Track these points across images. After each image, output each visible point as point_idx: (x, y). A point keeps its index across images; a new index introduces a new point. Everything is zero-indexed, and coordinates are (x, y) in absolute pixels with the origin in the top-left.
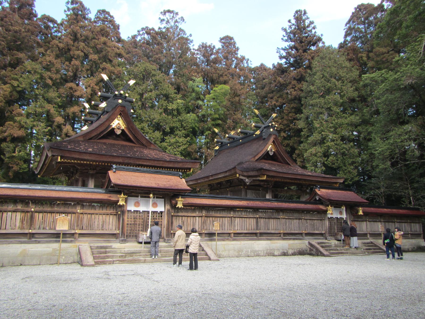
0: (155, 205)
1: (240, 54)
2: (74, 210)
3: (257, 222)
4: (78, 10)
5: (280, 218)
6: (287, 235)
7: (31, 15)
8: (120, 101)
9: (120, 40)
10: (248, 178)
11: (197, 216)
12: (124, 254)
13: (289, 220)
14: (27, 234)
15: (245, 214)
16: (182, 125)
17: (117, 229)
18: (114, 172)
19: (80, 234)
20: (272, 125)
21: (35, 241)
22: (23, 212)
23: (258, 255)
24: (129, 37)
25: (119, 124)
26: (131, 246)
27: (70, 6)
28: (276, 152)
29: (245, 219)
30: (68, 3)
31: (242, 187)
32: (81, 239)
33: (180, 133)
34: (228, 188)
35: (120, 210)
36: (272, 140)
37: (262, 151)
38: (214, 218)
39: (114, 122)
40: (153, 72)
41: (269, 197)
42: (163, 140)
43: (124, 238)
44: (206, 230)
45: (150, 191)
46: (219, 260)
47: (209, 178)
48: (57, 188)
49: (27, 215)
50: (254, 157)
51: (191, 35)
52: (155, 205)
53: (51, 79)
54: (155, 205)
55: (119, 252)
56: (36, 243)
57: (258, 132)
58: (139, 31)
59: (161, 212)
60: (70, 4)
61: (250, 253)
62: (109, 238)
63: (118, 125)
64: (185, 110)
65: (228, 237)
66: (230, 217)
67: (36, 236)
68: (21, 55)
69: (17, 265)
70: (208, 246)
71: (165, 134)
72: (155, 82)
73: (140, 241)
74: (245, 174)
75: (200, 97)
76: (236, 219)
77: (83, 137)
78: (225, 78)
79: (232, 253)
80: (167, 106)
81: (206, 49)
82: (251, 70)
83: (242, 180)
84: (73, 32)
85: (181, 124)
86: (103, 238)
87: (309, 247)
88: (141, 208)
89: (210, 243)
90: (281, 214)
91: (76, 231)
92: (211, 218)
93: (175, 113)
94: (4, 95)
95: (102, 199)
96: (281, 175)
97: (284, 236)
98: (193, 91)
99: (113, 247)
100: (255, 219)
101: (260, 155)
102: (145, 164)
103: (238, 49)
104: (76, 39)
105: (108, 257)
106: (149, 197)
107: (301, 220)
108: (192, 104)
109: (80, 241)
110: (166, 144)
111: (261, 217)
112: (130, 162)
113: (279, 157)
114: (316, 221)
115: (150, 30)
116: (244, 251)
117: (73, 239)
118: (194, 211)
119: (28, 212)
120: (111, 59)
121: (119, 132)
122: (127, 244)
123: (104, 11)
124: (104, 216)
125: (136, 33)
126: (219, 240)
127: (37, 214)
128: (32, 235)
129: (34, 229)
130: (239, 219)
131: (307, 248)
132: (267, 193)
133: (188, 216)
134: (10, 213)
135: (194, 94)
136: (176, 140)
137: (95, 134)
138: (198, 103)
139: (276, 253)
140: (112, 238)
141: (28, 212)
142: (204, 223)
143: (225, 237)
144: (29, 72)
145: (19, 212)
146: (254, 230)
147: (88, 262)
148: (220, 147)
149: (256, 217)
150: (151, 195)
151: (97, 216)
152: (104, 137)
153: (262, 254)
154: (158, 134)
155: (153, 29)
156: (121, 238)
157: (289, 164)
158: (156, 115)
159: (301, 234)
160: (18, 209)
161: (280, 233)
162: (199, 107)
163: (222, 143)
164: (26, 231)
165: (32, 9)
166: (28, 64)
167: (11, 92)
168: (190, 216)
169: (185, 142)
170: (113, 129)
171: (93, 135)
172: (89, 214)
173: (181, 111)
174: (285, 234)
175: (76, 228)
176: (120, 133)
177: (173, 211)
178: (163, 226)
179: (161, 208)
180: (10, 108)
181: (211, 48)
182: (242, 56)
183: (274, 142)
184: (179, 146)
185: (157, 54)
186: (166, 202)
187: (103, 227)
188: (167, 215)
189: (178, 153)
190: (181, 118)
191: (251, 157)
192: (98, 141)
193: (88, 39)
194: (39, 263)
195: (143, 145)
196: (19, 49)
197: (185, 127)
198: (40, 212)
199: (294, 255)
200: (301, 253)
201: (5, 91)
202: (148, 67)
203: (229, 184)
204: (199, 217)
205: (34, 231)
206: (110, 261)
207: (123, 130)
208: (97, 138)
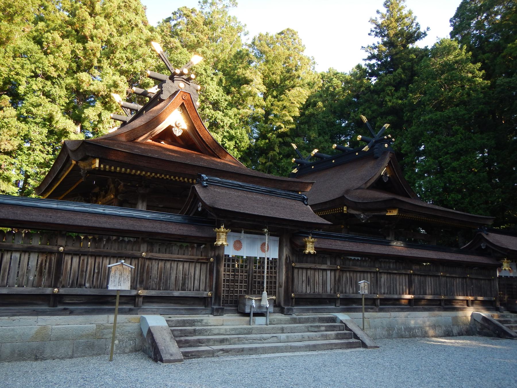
10: (363, 213)
11: (329, 270)
17: (208, 290)
20: (388, 137)
21: (65, 309)
24: (159, 23)
31: (343, 226)
32: (146, 306)
35: (213, 254)
43: (219, 305)
44: (342, 292)
48: (100, 210)
49: (51, 260)
55: (216, 332)
61: (403, 333)
62: (194, 304)
65: (372, 305)
66: (374, 272)
73: (247, 311)
83: (353, 215)
90: (441, 268)
97: (446, 304)
99: (205, 321)
106: (263, 234)
114: (483, 281)
117: (132, 307)
119: (51, 253)
124: (186, 265)
127: (68, 258)
129: (63, 287)
134: (17, 255)
140: (199, 305)
141: (51, 253)
142: (337, 282)
145: (35, 252)
147: (171, 355)
151: (174, 265)
156: (214, 304)
161: (440, 300)
163: (302, 164)
164: (49, 291)
168: (319, 269)
172: (162, 260)
175: (138, 286)
176: (180, 134)
178: (277, 285)
179: (273, 253)
183: (390, 163)
187: (184, 284)
198: (74, 254)
205: (62, 291)
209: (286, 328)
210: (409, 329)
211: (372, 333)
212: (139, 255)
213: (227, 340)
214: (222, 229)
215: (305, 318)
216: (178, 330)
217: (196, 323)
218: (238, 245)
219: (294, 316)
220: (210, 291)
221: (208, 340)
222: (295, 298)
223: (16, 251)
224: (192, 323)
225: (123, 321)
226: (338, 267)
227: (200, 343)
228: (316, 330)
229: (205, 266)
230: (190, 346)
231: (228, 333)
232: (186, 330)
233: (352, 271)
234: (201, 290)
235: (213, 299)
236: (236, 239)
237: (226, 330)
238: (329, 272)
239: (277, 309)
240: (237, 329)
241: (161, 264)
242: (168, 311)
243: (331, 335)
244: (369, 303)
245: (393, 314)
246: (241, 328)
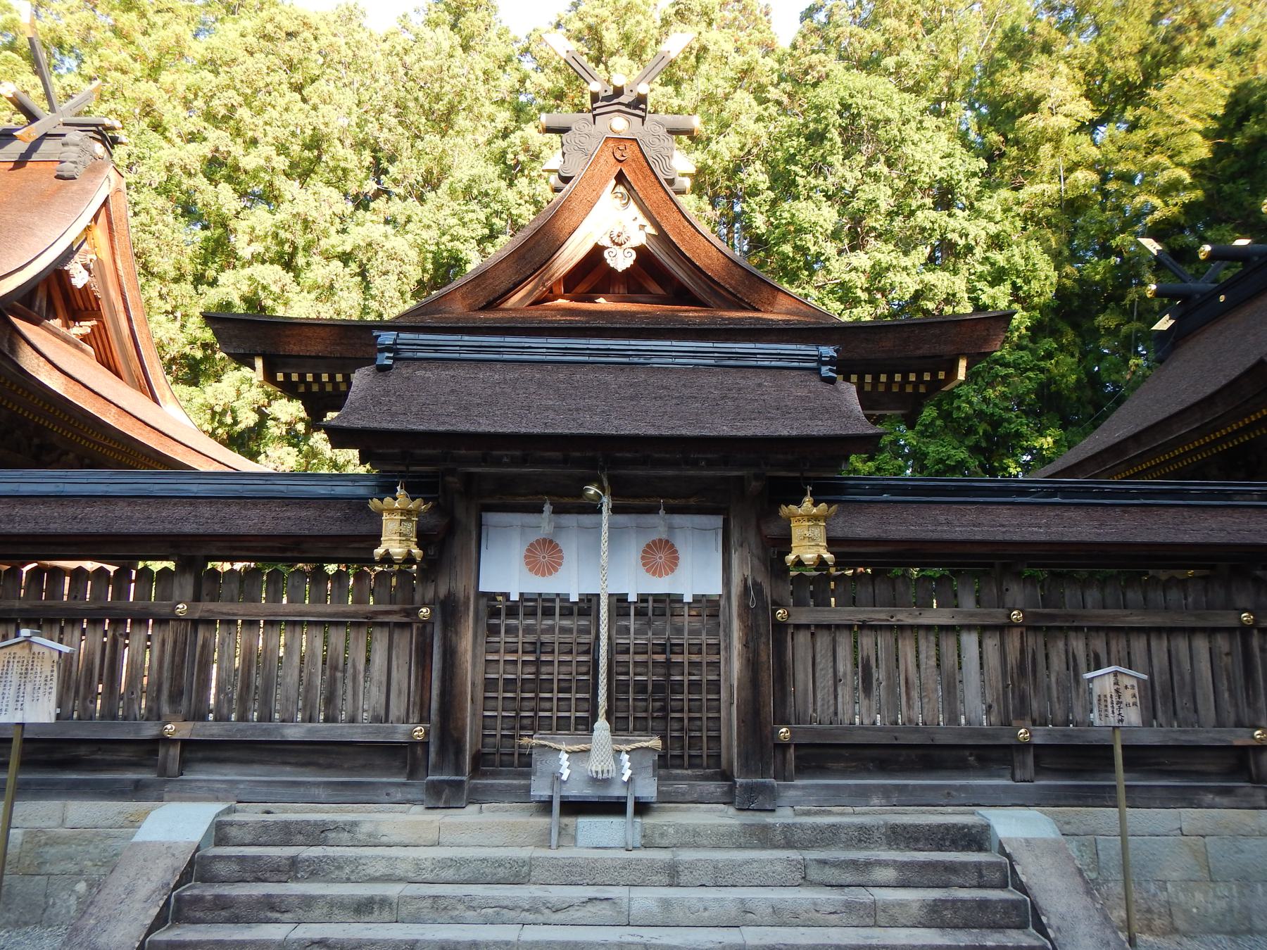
0: (661, 555)
11: (969, 628)
19: (186, 744)
26: (483, 829)
32: (200, 775)
35: (430, 594)
38: (1099, 644)
43: (458, 770)
54: (661, 555)
55: (380, 869)
59: (708, 607)
62: (367, 768)
65: (1232, 774)
66: (1230, 631)
86: (329, 766)
92: (1078, 645)
122: (469, 815)
126: (1137, 798)
133: (902, 628)
140: (388, 770)
156: (439, 768)
163: (1186, 297)
175: (166, 709)
178: (724, 695)
186: (734, 539)
187: (330, 700)
209: (692, 866)
211: (1222, 905)
212: (168, 610)
213: (384, 902)
215: (814, 828)
216: (229, 858)
217: (332, 835)
218: (544, 555)
219: (783, 817)
220: (421, 721)
221: (307, 902)
222: (796, 745)
224: (318, 834)
225: (110, 822)
226: (1016, 616)
227: (272, 908)
228: (848, 877)
229: (407, 634)
230: (235, 920)
231: (429, 877)
232: (259, 858)
233: (1097, 629)
234: (391, 717)
235: (432, 749)
237: (417, 864)
238: (970, 641)
239: (713, 787)
240: (467, 862)
242: (264, 789)
243: (902, 904)
244: (1212, 768)
246: (484, 860)
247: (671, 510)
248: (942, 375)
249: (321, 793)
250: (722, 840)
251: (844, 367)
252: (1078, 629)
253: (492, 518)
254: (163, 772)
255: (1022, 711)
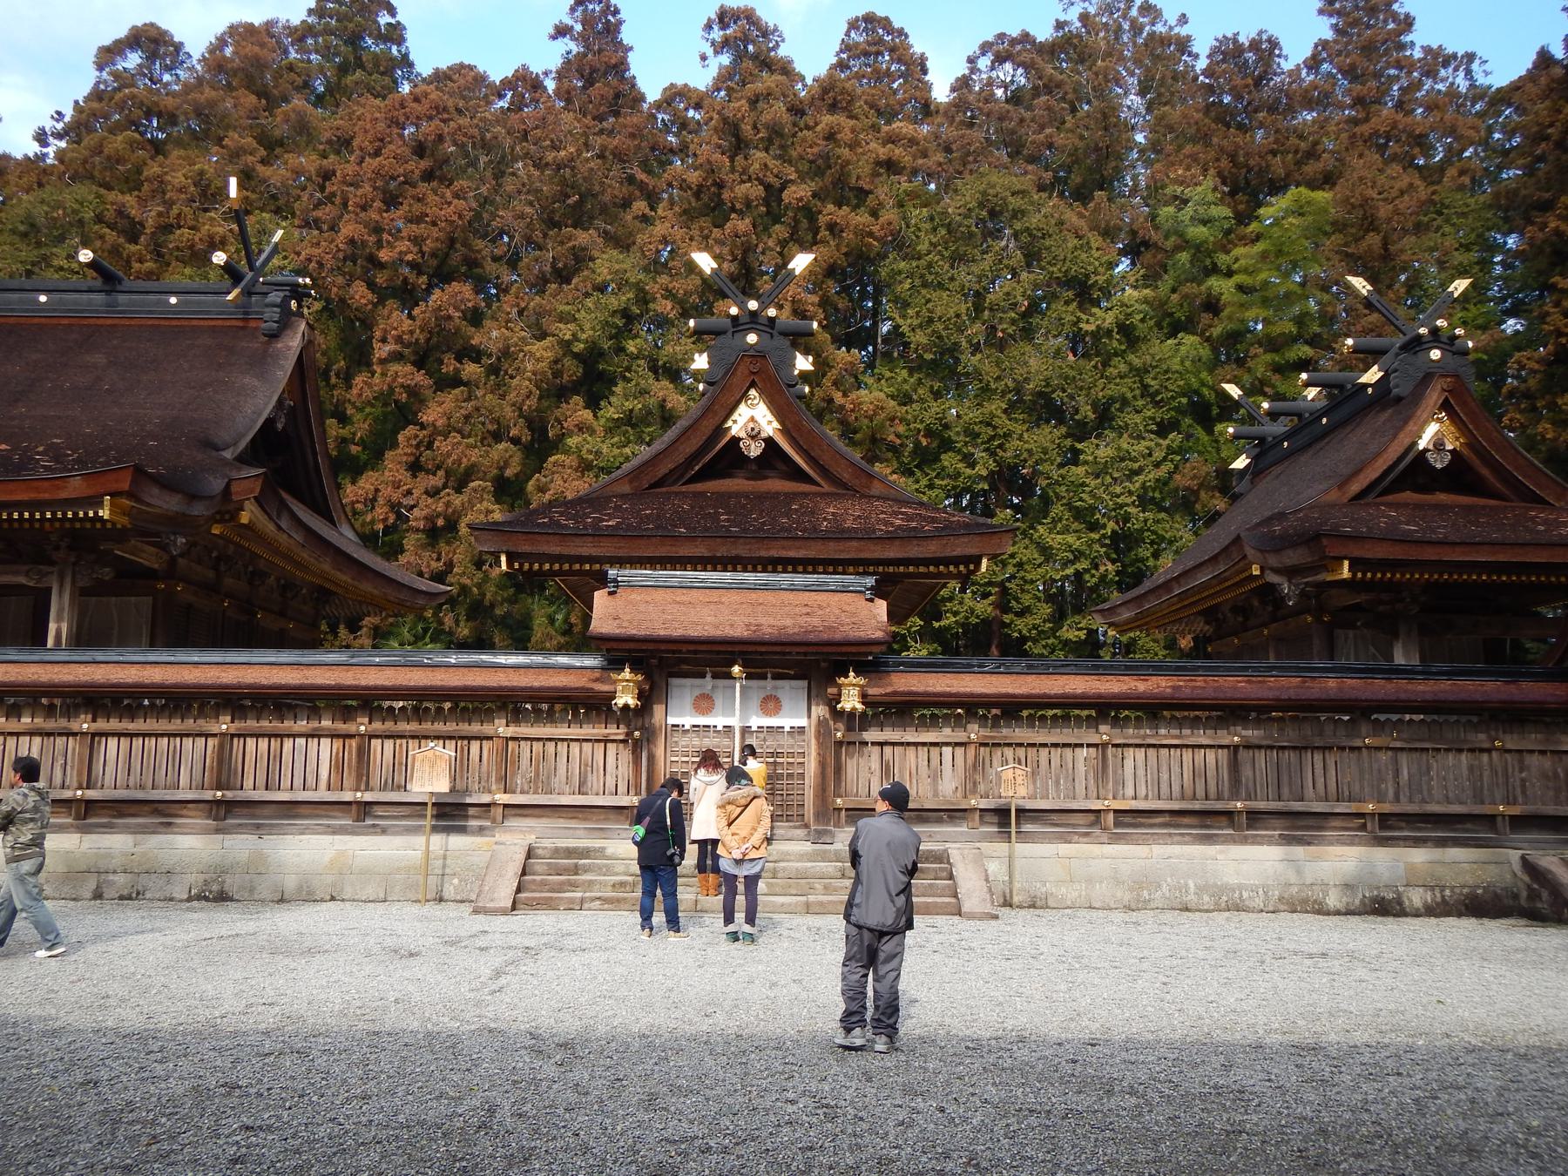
0: (771, 704)
1: (1421, 38)
2: (487, 729)
3: (1234, 766)
4: (746, 40)
5: (1359, 748)
6: (1387, 827)
7: (626, 97)
8: (752, 338)
9: (927, 109)
11: (947, 744)
12: (630, 879)
13: (1415, 755)
14: (349, 803)
15: (1175, 732)
16: (1145, 387)
18: (610, 593)
19: (505, 806)
22: (338, 736)
23: (1239, 908)
25: (752, 419)
27: (717, 34)
28: (1466, 452)
29: (1175, 753)
30: (708, 27)
32: (513, 822)
33: (1138, 419)
34: (1265, 625)
36: (1434, 396)
37: (1378, 455)
38: (1021, 752)
39: (735, 416)
40: (1015, 202)
41: (1406, 655)
42: (1074, 458)
45: (732, 653)
46: (996, 917)
47: (1170, 590)
50: (1342, 486)
51: (1183, 19)
52: (771, 705)
53: (669, 294)
55: (621, 869)
56: (375, 833)
57: (1372, 375)
58: (971, 61)
60: (716, 28)
61: (1192, 897)
63: (751, 425)
64: (1159, 325)
65: (1091, 825)
66: (1096, 746)
67: (379, 811)
68: (583, 237)
69: (322, 900)
70: (980, 859)
71: (1081, 432)
72: (1025, 238)
74: (1273, 561)
75: (1214, 265)
76: (1130, 752)
77: (631, 482)
78: (1327, 162)
79: (1101, 892)
80: (1079, 320)
81: (1247, 60)
82: (1503, 97)
84: (725, 120)
85: (1141, 382)
87: (1526, 878)
88: (719, 721)
89: (1001, 848)
91: (497, 797)
92: (1009, 752)
93: (1115, 344)
94: (534, 373)
95: (564, 689)
96: (1430, 554)
98: (1185, 244)
99: (609, 851)
100: (1223, 754)
101: (1372, 474)
102: (792, 554)
103: (1408, 23)
104: (739, 145)
105: (574, 886)
106: (729, 676)
107: (1485, 757)
108: (1185, 297)
109: (510, 830)
110: (1080, 470)
111: (1256, 742)
112: (734, 553)
113: (1485, 472)
115: (1014, 42)
116: (1165, 888)
118: (934, 722)
119: (351, 736)
120: (866, 187)
121: (755, 450)
123: (870, 19)
124: (587, 747)
125: (962, 69)
127: (376, 743)
128: (364, 810)
130: (1140, 753)
131: (1520, 884)
132: (1396, 636)
133: (909, 744)
134: (301, 741)
135: (1184, 257)
136: (1119, 449)
137: (671, 466)
138: (1210, 288)
139: (1333, 901)
140: (618, 822)
141: (351, 736)
143: (1074, 826)
144: (601, 288)
145: (326, 736)
146: (1219, 798)
148: (1255, 459)
149: (1225, 742)
150: (736, 669)
151: (562, 747)
152: (706, 474)
153: (1258, 902)
154: (1048, 436)
155: (1026, 37)
157: (1541, 501)
158: (1037, 363)
159: (1490, 820)
160: (323, 729)
162: (1212, 306)
163: (1262, 440)
164: (347, 796)
165: (623, 79)
166: (606, 263)
167: (556, 362)
168: (916, 744)
169: (1158, 455)
170: (736, 440)
171: (663, 470)
173: (1142, 330)
174: (1385, 820)
177: (841, 726)
180: (558, 413)
181: (1266, 49)
182: (1427, 50)
184: (1138, 472)
185: (1042, 128)
186: (813, 693)
188: (817, 738)
189: (1129, 500)
190: (1137, 362)
191: (1324, 486)
192: (684, 489)
193: (780, 134)
194: (382, 896)
195: (844, 486)
196: (579, 219)
197: (1158, 392)
199: (1436, 916)
200: (1480, 905)
201: (538, 360)
202: (993, 187)
203: (1270, 609)
204: (957, 744)
205: (368, 797)
206: (572, 900)
207: (769, 441)
208: (682, 476)
210: (1218, 890)
214: (627, 674)
223: (300, 736)
224: (585, 853)
236: (697, 692)
239: (801, 832)
241: (537, 746)
245: (1158, 850)
247: (776, 677)
248: (972, 567)
249: (581, 833)
250: (802, 857)
251: (878, 592)
252: (1009, 745)
253: (675, 681)
254: (494, 821)
255: (974, 791)
